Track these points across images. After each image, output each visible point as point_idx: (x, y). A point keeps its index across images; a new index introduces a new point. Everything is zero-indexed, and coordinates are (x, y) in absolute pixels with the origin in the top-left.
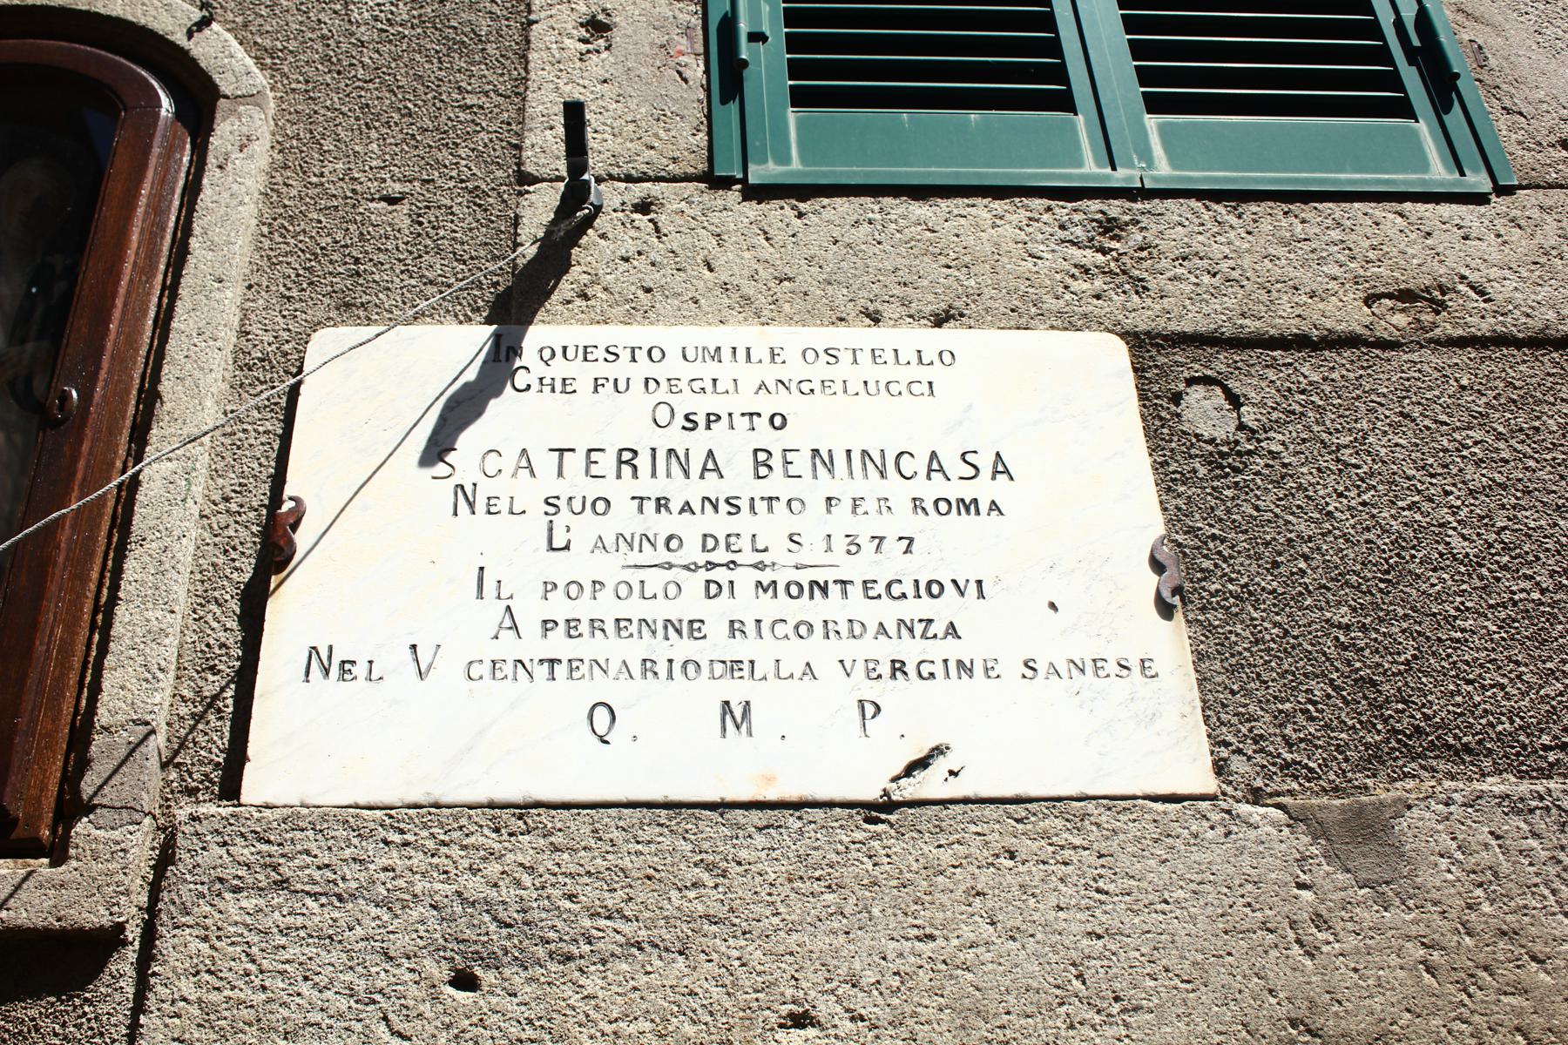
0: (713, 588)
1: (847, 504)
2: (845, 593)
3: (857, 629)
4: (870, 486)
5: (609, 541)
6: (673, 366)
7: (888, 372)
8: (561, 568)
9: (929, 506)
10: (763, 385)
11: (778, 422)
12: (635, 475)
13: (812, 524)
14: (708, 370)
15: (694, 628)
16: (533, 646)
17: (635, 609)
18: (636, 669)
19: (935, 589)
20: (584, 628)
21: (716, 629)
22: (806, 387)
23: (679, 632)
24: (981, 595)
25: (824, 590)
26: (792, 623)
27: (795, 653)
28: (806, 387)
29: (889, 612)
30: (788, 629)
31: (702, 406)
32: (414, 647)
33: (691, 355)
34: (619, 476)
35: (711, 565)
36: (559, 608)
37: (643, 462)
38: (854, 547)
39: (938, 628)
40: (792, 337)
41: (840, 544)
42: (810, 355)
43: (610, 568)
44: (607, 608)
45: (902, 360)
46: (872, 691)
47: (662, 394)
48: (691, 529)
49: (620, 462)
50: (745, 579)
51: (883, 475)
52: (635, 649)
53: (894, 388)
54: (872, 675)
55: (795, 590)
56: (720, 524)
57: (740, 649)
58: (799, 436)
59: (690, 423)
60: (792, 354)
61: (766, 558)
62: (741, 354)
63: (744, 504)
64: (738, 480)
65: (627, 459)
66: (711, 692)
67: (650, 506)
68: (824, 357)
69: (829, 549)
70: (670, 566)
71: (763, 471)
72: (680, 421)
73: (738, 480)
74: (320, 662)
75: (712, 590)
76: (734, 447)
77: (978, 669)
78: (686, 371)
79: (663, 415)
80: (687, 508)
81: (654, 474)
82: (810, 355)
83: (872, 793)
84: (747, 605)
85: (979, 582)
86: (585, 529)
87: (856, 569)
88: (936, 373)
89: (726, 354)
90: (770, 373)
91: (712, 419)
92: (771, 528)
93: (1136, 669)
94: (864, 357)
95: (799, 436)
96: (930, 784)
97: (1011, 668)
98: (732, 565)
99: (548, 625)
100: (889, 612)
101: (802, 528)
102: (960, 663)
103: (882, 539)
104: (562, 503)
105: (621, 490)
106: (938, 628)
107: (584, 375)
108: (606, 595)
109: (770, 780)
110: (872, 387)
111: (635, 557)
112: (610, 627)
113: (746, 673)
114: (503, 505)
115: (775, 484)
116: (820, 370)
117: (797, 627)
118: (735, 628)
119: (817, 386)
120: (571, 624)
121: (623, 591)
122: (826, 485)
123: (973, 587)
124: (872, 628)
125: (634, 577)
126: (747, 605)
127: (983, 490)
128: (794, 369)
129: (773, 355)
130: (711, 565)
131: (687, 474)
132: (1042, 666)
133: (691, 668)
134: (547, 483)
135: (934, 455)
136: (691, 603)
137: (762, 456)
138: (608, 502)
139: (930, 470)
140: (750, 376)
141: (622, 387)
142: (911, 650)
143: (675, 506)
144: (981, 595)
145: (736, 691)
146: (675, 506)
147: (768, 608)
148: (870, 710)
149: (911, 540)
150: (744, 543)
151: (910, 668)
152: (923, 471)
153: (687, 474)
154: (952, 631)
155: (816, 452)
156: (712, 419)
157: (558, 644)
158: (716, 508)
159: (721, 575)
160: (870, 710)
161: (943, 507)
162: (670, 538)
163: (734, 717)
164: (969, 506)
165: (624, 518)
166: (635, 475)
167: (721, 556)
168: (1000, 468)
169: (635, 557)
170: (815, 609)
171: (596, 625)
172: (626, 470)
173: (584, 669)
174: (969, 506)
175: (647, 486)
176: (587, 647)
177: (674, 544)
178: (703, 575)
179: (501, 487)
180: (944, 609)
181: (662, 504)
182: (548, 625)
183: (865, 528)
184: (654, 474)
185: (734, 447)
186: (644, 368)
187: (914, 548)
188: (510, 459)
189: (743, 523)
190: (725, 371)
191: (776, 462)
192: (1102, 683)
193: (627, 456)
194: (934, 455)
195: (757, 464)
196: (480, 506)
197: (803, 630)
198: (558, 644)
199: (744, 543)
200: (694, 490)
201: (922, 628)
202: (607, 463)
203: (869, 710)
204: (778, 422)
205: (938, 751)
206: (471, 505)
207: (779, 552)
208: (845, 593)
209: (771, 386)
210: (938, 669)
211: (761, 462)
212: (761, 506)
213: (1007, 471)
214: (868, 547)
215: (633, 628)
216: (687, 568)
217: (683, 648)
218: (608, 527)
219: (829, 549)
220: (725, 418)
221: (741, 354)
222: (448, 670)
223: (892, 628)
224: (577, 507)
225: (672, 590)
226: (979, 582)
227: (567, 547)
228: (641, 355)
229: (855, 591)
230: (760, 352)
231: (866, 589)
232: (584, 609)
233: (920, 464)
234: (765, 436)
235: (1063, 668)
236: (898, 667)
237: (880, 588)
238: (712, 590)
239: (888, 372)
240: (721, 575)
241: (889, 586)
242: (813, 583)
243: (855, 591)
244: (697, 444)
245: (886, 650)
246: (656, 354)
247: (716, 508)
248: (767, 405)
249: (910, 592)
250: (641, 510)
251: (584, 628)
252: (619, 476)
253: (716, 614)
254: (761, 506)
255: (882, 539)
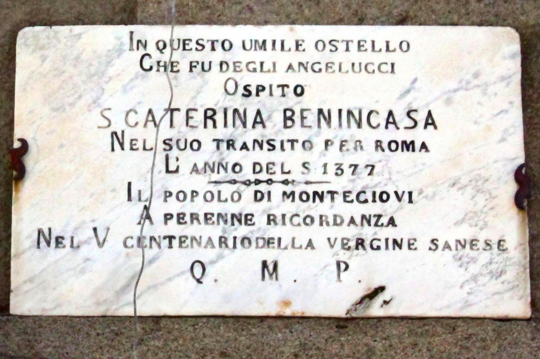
0: (259, 195)
1: (337, 144)
2: (333, 199)
3: (339, 221)
4: (351, 132)
5: (200, 166)
6: (237, 54)
7: (367, 57)
8: (174, 184)
9: (385, 145)
10: (290, 67)
11: (299, 91)
12: (215, 126)
13: (315, 157)
14: (258, 56)
15: (247, 219)
16: (159, 229)
17: (215, 207)
18: (216, 242)
19: (385, 197)
20: (188, 218)
21: (260, 220)
22: (316, 67)
23: (240, 221)
24: (411, 201)
25: (321, 199)
26: (303, 216)
27: (303, 234)
28: (316, 67)
29: (357, 210)
30: (300, 220)
31: (254, 80)
32: (95, 229)
33: (248, 46)
34: (205, 126)
35: (258, 182)
36: (174, 206)
37: (219, 117)
38: (340, 170)
39: (384, 220)
40: (309, 33)
41: (332, 169)
42: (320, 45)
43: (201, 183)
44: (200, 207)
45: (377, 48)
46: (344, 256)
47: (230, 73)
48: (246, 160)
49: (206, 117)
50: (277, 190)
51: (359, 125)
52: (215, 231)
53: (370, 68)
54: (345, 246)
55: (305, 197)
56: (263, 156)
57: (274, 232)
58: (311, 102)
59: (247, 93)
60: (309, 45)
61: (289, 177)
62: (278, 45)
63: (278, 145)
64: (274, 129)
65: (210, 116)
66: (256, 255)
67: (224, 146)
68: (328, 47)
69: (325, 173)
70: (234, 182)
71: (289, 123)
72: (241, 90)
73: (274, 129)
74: (45, 238)
75: (258, 197)
76: (273, 106)
77: (405, 245)
78: (244, 57)
79: (231, 87)
80: (244, 147)
81: (225, 125)
82: (320, 45)
83: (340, 311)
84: (279, 206)
85: (410, 193)
86: (187, 159)
87: (339, 184)
88: (397, 57)
89: (269, 45)
90: (295, 58)
91: (260, 89)
92: (292, 159)
93: (495, 246)
94: (353, 47)
95: (311, 102)
96: (376, 309)
97: (423, 244)
98: (269, 182)
99: (168, 217)
100: (357, 210)
101: (307, 162)
102: (395, 241)
103: (356, 166)
104: (173, 143)
105: (206, 135)
106: (384, 220)
107: (183, 59)
108: (199, 199)
109: (287, 303)
110: (357, 68)
111: (215, 177)
112: (202, 218)
113: (276, 245)
114: (140, 145)
115: (297, 132)
116: (325, 56)
117: (305, 219)
118: (271, 219)
119: (323, 66)
120: (181, 217)
121: (209, 196)
122: (327, 133)
123: (406, 197)
124: (347, 220)
125: (215, 189)
126: (279, 206)
127: (419, 135)
128: (310, 55)
129: (298, 45)
130: (258, 182)
131: (244, 124)
132: (441, 244)
133: (246, 242)
134: (165, 132)
135: (391, 113)
136: (246, 205)
137: (289, 114)
138: (199, 143)
139: (388, 122)
140: (284, 59)
141: (206, 67)
142: (368, 233)
143: (238, 145)
144: (411, 201)
145: (270, 255)
146: (238, 145)
147: (290, 207)
148: (343, 266)
149: (373, 167)
150: (277, 169)
151: (367, 244)
152: (383, 123)
153: (244, 124)
154: (392, 222)
155: (320, 111)
156: (260, 89)
157: (173, 228)
158: (261, 147)
159: (263, 187)
160: (343, 266)
161: (393, 146)
162: (235, 165)
163: (269, 269)
164: (409, 146)
165: (208, 153)
166: (215, 126)
167: (264, 176)
168: (430, 121)
169: (215, 177)
170: (317, 209)
171: (194, 217)
172: (210, 122)
173: (188, 242)
174: (409, 146)
175: (221, 133)
176: (191, 230)
177: (237, 169)
178: (253, 188)
179: (139, 133)
180: (391, 207)
181: (230, 144)
182: (168, 217)
183: (348, 159)
184: (225, 125)
185: (273, 106)
186: (219, 55)
187: (375, 171)
188: (142, 116)
189: (277, 156)
190: (267, 56)
191: (297, 118)
192: (473, 254)
193: (210, 113)
194: (391, 113)
195: (286, 118)
196: (127, 145)
197: (308, 220)
198: (173, 228)
199: (277, 169)
200: (251, 135)
201: (376, 220)
202: (198, 117)
203: (342, 267)
204: (299, 91)
205: (381, 289)
206: (122, 145)
207: (297, 175)
208: (333, 199)
209: (295, 66)
210: (382, 244)
211: (288, 118)
212: (287, 146)
213: (433, 123)
214: (348, 171)
215: (215, 219)
216: (244, 183)
217: (242, 230)
218: (200, 158)
219: (325, 173)
220: (267, 90)
221: (278, 45)
222: (114, 242)
223: (358, 220)
224: (182, 146)
225: (236, 196)
226: (410, 193)
227: (177, 171)
228: (218, 46)
229: (339, 198)
230: (290, 44)
231: (345, 197)
232: (188, 208)
233: (380, 119)
234: (291, 101)
235: (453, 244)
236: (360, 243)
237: (353, 196)
238: (258, 197)
239: (367, 57)
240: (263, 187)
241: (358, 196)
242: (315, 193)
243: (339, 198)
244: (251, 106)
245: (351, 233)
246: (227, 45)
247: (261, 147)
248: (292, 79)
249: (370, 199)
250: (218, 147)
251: (188, 218)
252: (205, 126)
253: (258, 210)
254: (287, 146)
255: (356, 166)
